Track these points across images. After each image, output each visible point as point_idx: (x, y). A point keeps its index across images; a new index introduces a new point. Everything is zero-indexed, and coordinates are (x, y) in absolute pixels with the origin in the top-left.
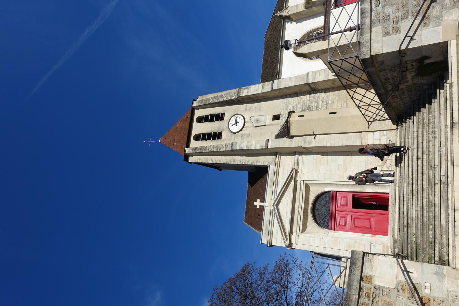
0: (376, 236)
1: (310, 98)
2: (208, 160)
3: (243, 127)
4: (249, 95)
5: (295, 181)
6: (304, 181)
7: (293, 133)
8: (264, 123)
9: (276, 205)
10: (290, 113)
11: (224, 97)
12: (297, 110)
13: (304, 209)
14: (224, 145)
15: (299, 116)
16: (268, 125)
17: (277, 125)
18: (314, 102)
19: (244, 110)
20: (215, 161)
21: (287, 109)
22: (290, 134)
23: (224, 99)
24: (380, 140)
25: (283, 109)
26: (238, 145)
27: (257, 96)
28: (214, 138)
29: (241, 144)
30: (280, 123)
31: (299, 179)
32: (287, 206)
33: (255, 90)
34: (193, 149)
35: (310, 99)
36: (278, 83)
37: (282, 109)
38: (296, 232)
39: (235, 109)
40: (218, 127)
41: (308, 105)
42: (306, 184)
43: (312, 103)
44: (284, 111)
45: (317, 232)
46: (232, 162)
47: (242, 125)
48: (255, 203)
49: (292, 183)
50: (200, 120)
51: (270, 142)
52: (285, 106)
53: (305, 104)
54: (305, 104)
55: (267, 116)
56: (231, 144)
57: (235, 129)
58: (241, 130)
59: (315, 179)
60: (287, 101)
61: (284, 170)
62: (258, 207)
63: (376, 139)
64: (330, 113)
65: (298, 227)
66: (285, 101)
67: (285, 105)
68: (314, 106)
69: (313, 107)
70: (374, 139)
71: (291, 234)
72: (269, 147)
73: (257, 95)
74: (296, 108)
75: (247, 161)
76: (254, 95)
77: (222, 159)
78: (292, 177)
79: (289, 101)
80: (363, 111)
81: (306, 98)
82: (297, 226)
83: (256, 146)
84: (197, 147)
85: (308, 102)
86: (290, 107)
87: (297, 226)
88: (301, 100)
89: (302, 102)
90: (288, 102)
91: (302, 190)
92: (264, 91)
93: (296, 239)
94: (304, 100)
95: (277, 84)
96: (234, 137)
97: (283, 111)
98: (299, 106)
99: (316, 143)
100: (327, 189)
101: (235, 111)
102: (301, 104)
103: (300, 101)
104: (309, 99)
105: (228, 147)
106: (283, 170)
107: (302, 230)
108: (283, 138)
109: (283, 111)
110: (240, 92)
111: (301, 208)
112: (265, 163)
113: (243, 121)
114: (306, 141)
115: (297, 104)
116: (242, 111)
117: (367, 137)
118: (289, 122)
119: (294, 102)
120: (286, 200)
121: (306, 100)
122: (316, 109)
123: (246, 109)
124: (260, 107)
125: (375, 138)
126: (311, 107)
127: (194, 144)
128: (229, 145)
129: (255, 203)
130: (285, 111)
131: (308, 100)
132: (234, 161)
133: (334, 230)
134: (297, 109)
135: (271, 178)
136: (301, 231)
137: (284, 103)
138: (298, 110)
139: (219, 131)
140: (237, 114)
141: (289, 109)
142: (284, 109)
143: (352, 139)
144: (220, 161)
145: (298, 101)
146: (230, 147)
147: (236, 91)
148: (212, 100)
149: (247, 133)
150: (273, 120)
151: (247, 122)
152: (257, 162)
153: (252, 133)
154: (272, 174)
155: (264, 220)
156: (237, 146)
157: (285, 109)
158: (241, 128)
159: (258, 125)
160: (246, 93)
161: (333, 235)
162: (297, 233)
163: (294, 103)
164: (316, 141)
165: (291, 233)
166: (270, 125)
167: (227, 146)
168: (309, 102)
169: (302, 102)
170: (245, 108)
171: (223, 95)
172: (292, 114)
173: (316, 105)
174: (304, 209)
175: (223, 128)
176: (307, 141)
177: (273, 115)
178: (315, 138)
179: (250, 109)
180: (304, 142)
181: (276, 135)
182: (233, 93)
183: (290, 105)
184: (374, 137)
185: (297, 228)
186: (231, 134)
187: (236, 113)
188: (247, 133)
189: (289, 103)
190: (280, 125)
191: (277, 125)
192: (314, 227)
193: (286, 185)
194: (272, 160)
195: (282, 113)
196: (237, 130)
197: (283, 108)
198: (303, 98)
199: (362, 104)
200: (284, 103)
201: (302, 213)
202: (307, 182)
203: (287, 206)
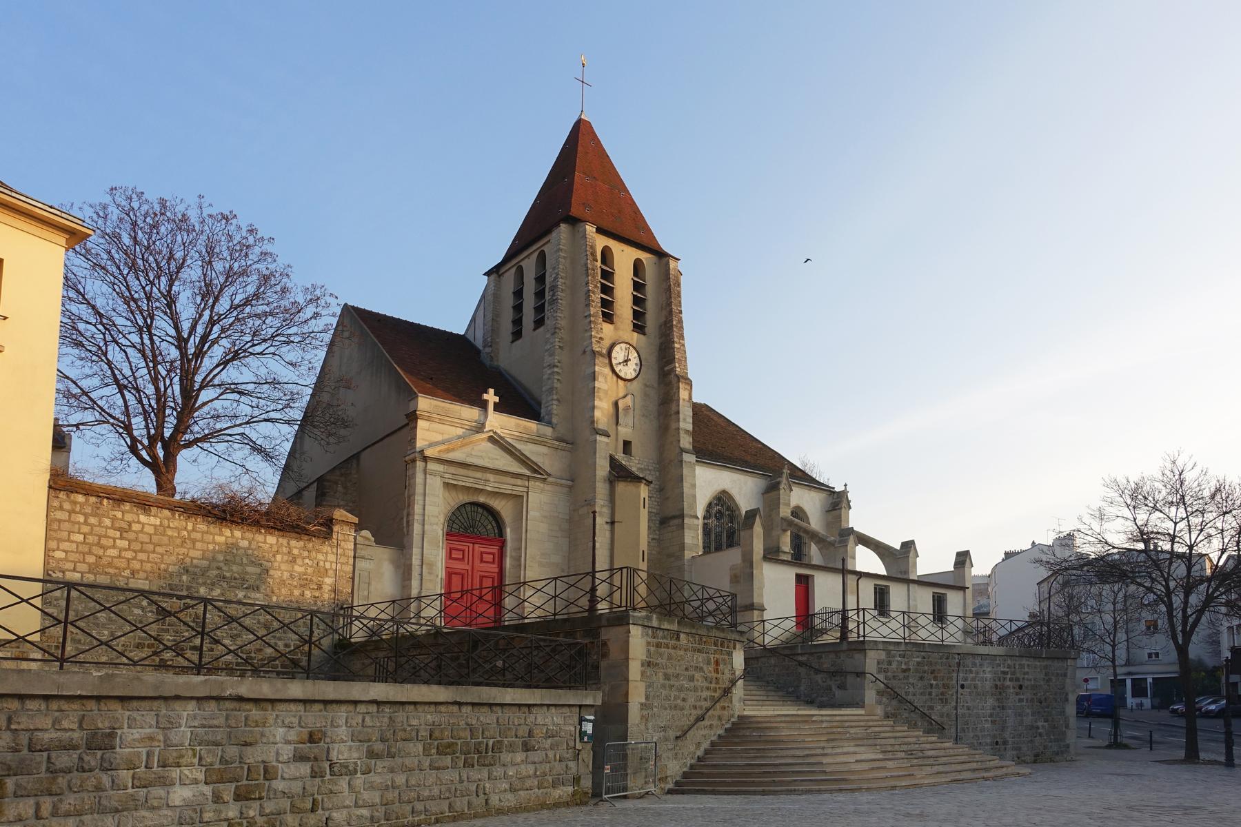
3: (618, 376)
4: (678, 400)
6: (527, 493)
7: (621, 487)
27: (671, 415)
31: (532, 483)
36: (690, 462)
47: (622, 375)
48: (491, 391)
49: (524, 471)
55: (630, 430)
59: (531, 513)
62: (485, 396)
72: (599, 438)
73: (673, 417)
76: (678, 413)
78: (535, 471)
92: (682, 435)
95: (689, 458)
100: (509, 533)
113: (629, 377)
120: (498, 457)
129: (491, 391)
132: (560, 347)
136: (447, 481)
166: (617, 434)
191: (616, 448)
201: (477, 486)
203: (489, 458)
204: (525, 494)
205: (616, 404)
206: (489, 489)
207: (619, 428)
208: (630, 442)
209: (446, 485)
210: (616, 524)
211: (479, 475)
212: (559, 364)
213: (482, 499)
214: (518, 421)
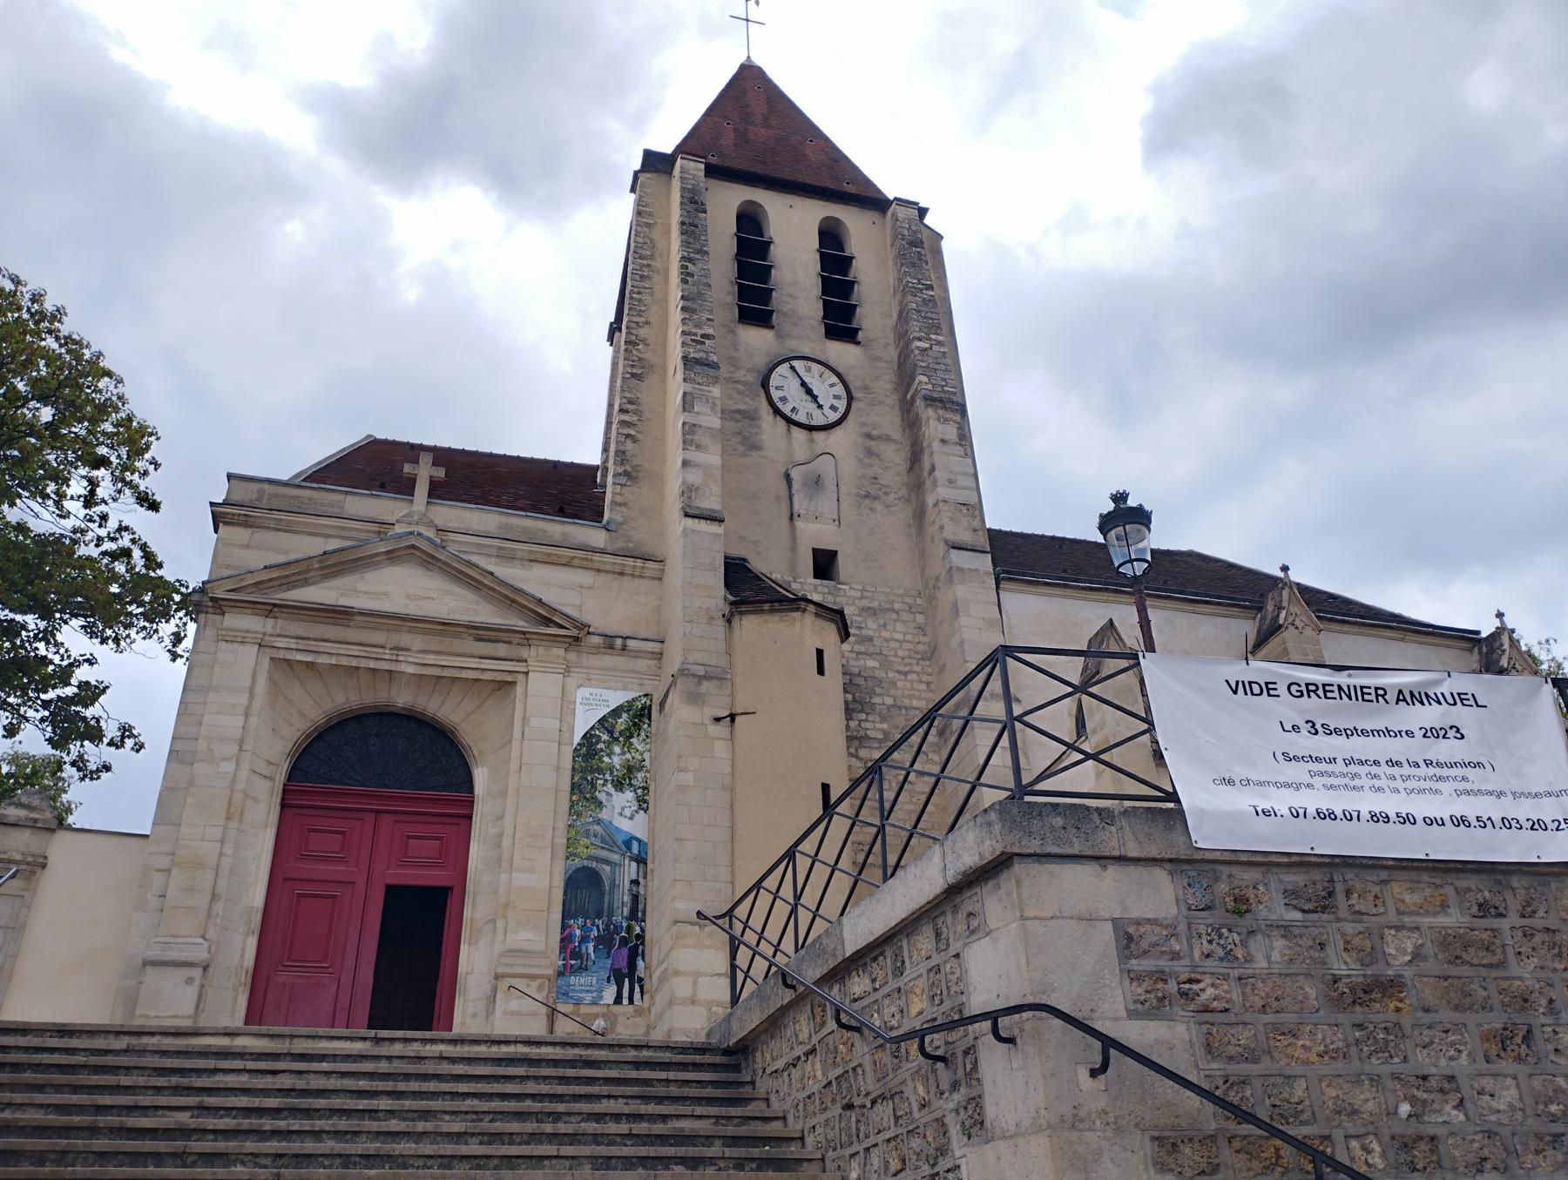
0: (241, 989)
1: (904, 711)
2: (645, 262)
3: (790, 421)
4: (930, 446)
5: (528, 636)
7: (750, 625)
8: (802, 512)
9: (413, 547)
10: (837, 618)
11: (930, 339)
12: (854, 655)
13: (391, 671)
14: (710, 331)
15: (820, 653)
16: (793, 527)
17: (793, 567)
18: (885, 726)
19: (865, 430)
20: (639, 293)
21: (863, 613)
22: (741, 613)
23: (919, 339)
24: (693, 1001)
25: (863, 597)
26: (704, 388)
27: (924, 483)
28: (743, 293)
29: (708, 401)
30: (803, 580)
32: (408, 597)
33: (951, 472)
34: (695, 194)
35: (904, 711)
37: (864, 590)
38: (278, 631)
39: (876, 390)
40: (794, 311)
41: (873, 701)
42: (513, 683)
43: (883, 720)
44: (854, 598)
45: (273, 730)
46: (633, 366)
50: (831, 237)
51: (714, 528)
52: (875, 604)
53: (878, 690)
54: (878, 690)
55: (832, 528)
56: (715, 358)
57: (784, 384)
58: (777, 412)
59: (534, 722)
60: (898, 614)
61: (584, 591)
63: (695, 983)
64: (828, 786)
65: (300, 641)
66: (896, 606)
67: (880, 605)
68: (868, 725)
69: (866, 720)
70: (696, 976)
71: (270, 608)
73: (928, 483)
74: (862, 649)
75: (633, 433)
76: (933, 469)
77: (647, 323)
78: (548, 622)
79: (896, 620)
80: (771, 882)
81: (907, 692)
82: (309, 639)
83: (698, 465)
84: (705, 212)
85: (889, 701)
86: (872, 624)
87: (309, 639)
88: (899, 672)
89: (891, 675)
90: (894, 616)
91: (482, 666)
93: (244, 635)
94: (900, 684)
96: (743, 379)
97: (852, 593)
98: (871, 663)
99: (694, 724)
101: (866, 388)
102: (880, 674)
103: (896, 667)
104: (900, 708)
105: (698, 347)
106: (581, 587)
107: (288, 662)
108: (727, 585)
109: (852, 593)
110: (945, 408)
111: (394, 658)
112: (618, 508)
114: (705, 682)
115: (881, 654)
116: (863, 420)
117: (708, 947)
118: (797, 610)
119: (893, 644)
120: (431, 594)
121: (899, 693)
122: (855, 733)
123: (868, 436)
124: (876, 498)
125: (702, 980)
126: (867, 714)
127: (726, 201)
128: (706, 352)
130: (853, 604)
131: (899, 704)
132: (633, 375)
133: (283, 805)
134: (860, 653)
135: (545, 531)
136: (281, 654)
137: (891, 602)
138: (852, 659)
139: (777, 318)
140: (850, 398)
141: (860, 619)
142: (864, 601)
143: (706, 880)
144: (641, 316)
145: (893, 659)
146: (697, 356)
147: (955, 394)
148: (920, 286)
149: (763, 437)
150: (814, 550)
151: (812, 441)
152: (626, 474)
153: (760, 456)
154: (565, 535)
155: (347, 493)
156: (699, 384)
157: (865, 603)
158: (786, 409)
159: (795, 486)
160: (941, 436)
161: (256, 800)
162: (271, 635)
163: (887, 641)
164: (703, 724)
165: (272, 610)
167: (704, 343)
168: (889, 708)
169: (891, 675)
170: (875, 433)
171: (940, 338)
172: (833, 627)
173: (872, 734)
174: (390, 672)
175: (788, 336)
176: (706, 686)
177: (836, 553)
178: (718, 720)
179: (870, 453)
180: (702, 673)
181: (745, 560)
182: (945, 380)
183: (879, 625)
184: (705, 975)
185: (297, 638)
186: (762, 367)
187: (855, 394)
188: (763, 437)
189: (891, 619)
190: (791, 579)
191: (793, 567)
192: (301, 714)
193: (511, 598)
194: (630, 541)
195: (844, 590)
196: (776, 395)
197: (870, 594)
198: (906, 680)
199: (803, 863)
200: (891, 602)
201: (372, 664)
202: (519, 689)
203: (408, 597)
204: (520, 677)
205: (788, 475)
206: (410, 669)
207: (799, 524)
208: (834, 554)
209: (284, 665)
210: (738, 719)
211: (379, 637)
212: (630, 407)
213: (402, 698)
214: (504, 519)
